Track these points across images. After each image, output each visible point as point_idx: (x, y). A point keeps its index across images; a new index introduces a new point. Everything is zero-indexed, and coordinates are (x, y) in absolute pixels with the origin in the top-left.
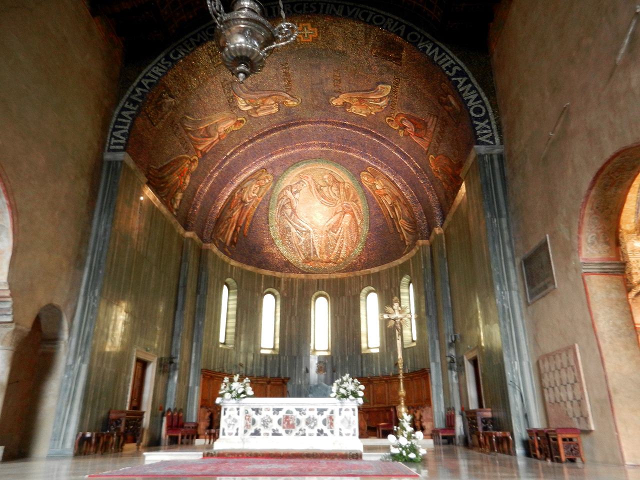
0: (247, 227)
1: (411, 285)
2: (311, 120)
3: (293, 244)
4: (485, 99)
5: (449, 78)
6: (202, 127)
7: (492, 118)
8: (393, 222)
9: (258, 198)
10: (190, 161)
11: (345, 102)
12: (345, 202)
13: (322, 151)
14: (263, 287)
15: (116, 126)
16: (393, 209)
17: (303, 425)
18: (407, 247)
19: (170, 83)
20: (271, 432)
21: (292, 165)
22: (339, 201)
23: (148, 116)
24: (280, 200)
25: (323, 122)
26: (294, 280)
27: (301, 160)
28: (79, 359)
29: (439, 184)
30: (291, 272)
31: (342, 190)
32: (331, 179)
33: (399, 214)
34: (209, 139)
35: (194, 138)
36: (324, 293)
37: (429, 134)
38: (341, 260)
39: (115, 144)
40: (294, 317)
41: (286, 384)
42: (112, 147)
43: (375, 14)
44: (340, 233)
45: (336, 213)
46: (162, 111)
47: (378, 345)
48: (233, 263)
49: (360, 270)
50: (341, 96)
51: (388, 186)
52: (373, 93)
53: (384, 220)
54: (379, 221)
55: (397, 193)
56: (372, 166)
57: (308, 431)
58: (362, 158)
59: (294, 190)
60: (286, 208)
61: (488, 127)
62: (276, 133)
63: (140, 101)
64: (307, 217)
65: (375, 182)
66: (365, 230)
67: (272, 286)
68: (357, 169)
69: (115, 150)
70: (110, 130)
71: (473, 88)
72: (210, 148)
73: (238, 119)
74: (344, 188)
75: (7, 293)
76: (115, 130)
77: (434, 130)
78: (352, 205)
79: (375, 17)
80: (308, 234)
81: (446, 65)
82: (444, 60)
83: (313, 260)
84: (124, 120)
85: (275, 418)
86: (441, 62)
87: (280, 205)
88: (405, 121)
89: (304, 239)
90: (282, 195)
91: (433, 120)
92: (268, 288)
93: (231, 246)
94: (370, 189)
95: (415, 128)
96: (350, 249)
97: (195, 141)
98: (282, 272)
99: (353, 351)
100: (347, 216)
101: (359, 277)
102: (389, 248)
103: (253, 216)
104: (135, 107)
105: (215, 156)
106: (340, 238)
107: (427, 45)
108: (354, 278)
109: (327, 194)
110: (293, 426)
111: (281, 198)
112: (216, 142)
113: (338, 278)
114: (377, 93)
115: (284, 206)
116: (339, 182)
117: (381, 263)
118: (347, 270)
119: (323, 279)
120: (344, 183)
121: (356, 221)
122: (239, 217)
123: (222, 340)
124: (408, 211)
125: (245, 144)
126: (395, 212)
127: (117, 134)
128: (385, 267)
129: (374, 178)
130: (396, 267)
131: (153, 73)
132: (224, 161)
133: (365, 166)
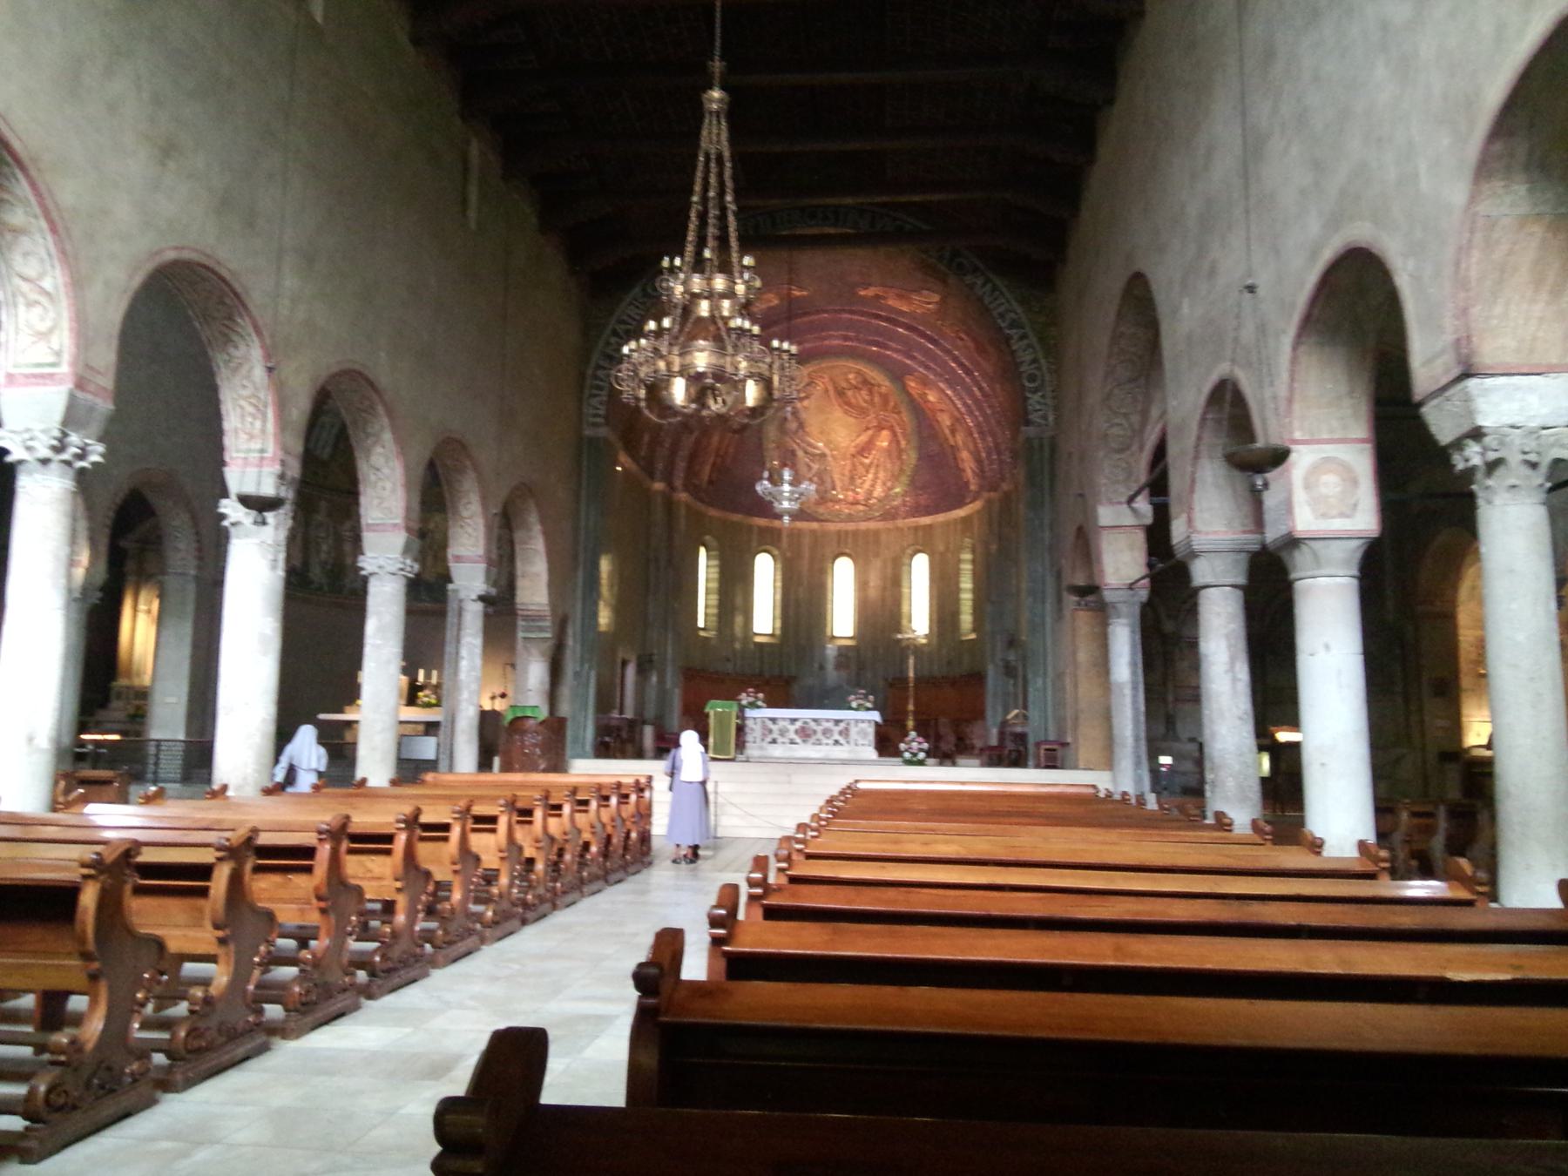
4: (1043, 361)
7: (1049, 389)
12: (882, 413)
16: (953, 431)
17: (819, 736)
20: (786, 740)
28: (586, 666)
45: (868, 429)
48: (713, 512)
49: (904, 518)
50: (872, 289)
55: (956, 413)
57: (825, 741)
61: (1042, 401)
71: (1030, 346)
75: (548, 613)
78: (893, 419)
81: (1001, 309)
82: (998, 302)
84: (601, 383)
85: (792, 728)
86: (991, 306)
100: (885, 433)
101: (902, 530)
109: (853, 401)
110: (808, 736)
119: (847, 532)
121: (898, 443)
123: (701, 624)
127: (594, 401)
128: (941, 518)
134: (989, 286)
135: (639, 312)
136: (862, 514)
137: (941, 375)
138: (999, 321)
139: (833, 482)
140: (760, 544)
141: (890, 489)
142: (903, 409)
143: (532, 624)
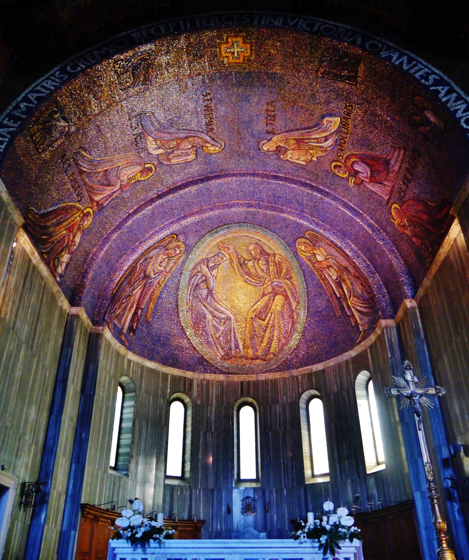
0: (150, 311)
1: (371, 383)
2: (235, 172)
3: (208, 335)
5: (426, 88)
6: (100, 170)
8: (340, 303)
9: (165, 273)
10: (83, 213)
11: (280, 146)
12: (275, 280)
13: (248, 213)
14: (169, 391)
16: (339, 285)
18: (362, 333)
19: (63, 100)
21: (209, 232)
22: (268, 279)
23: (32, 138)
24: (192, 278)
25: (251, 175)
26: (211, 383)
27: (220, 225)
29: (407, 242)
30: (205, 372)
31: (272, 264)
32: (259, 250)
33: (348, 291)
34: (108, 188)
35: (90, 184)
36: (250, 400)
37: (392, 175)
38: (272, 355)
40: (210, 433)
41: (200, 531)
43: (322, 23)
44: (269, 320)
45: (264, 295)
46: (51, 137)
47: (327, 471)
48: (131, 356)
49: (297, 368)
51: (332, 255)
52: (317, 130)
53: (328, 301)
54: (321, 303)
55: (345, 263)
56: (312, 230)
58: (298, 220)
59: (211, 265)
60: (200, 288)
62: (193, 189)
64: (226, 300)
65: (315, 252)
66: (302, 315)
67: (182, 390)
68: (291, 235)
72: (109, 200)
73: (146, 166)
74: (274, 262)
77: (400, 167)
79: (323, 27)
80: (228, 322)
83: (234, 357)
86: (412, 71)
87: (193, 284)
88: (358, 164)
89: (223, 328)
90: (196, 271)
91: (398, 155)
92: (175, 393)
93: (129, 333)
94: (308, 261)
95: (371, 172)
96: (284, 341)
97: (91, 187)
98: (194, 371)
99: (293, 481)
100: (279, 298)
101: (297, 377)
102: (335, 337)
103: (159, 297)
104: (16, 123)
105: (114, 213)
106: (270, 325)
107: (391, 54)
108: (290, 379)
109: (253, 271)
111: (194, 275)
112: (117, 194)
113: (268, 380)
114: (321, 130)
115: (197, 285)
116: (268, 254)
117: (326, 358)
118: (279, 369)
119: (249, 382)
120: (274, 255)
121: (290, 304)
122: (140, 298)
124: (361, 284)
125: (152, 201)
126: (342, 288)
128: (332, 362)
129: (314, 246)
130: (347, 362)
132: (126, 220)
133: (302, 230)
134: (405, 58)
135: (54, 84)
136: (261, 367)
137: (329, 230)
138: (423, 81)
139: (237, 341)
140: (173, 392)
141: (284, 345)
142: (293, 275)
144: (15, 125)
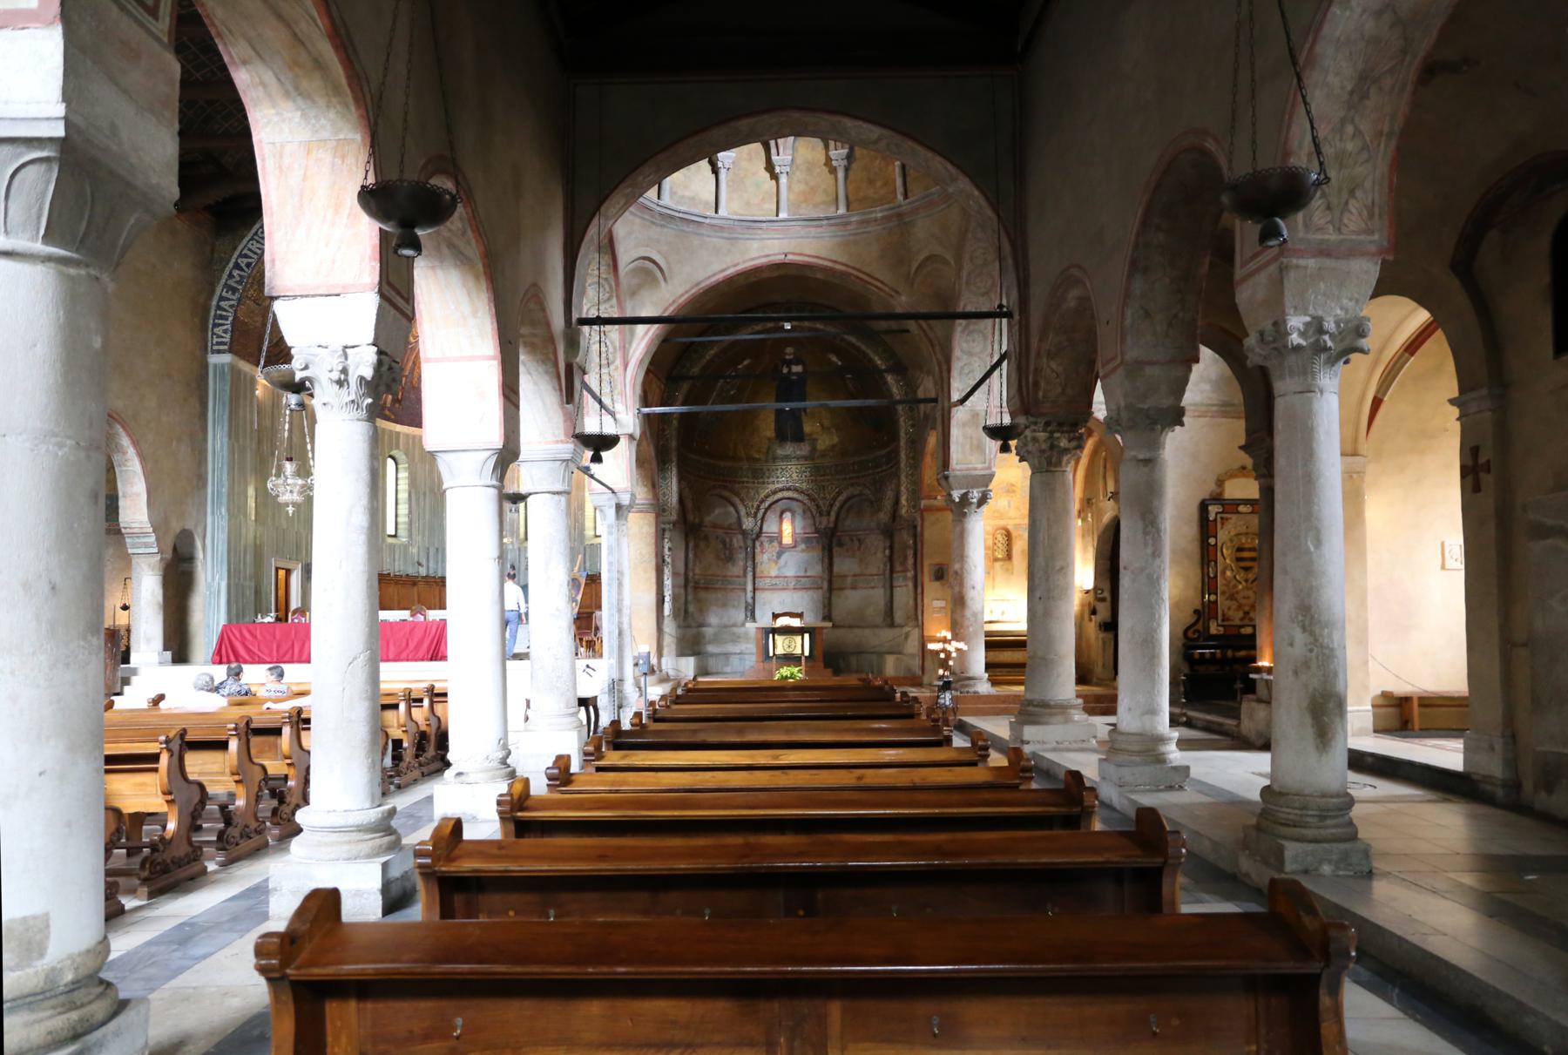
15: (216, 321)
39: (218, 343)
42: (215, 348)
63: (240, 287)
69: (219, 352)
70: (210, 326)
76: (215, 325)
84: (224, 313)
127: (218, 330)
131: (250, 250)
143: (137, 540)
144: (234, 298)
